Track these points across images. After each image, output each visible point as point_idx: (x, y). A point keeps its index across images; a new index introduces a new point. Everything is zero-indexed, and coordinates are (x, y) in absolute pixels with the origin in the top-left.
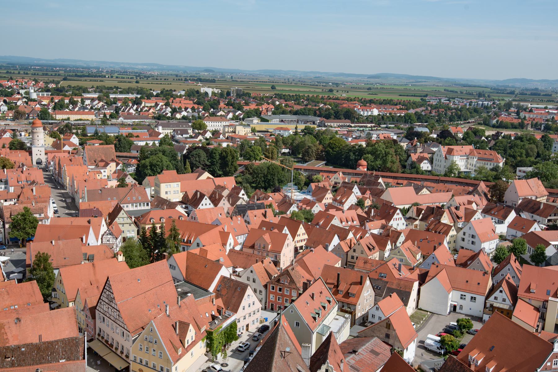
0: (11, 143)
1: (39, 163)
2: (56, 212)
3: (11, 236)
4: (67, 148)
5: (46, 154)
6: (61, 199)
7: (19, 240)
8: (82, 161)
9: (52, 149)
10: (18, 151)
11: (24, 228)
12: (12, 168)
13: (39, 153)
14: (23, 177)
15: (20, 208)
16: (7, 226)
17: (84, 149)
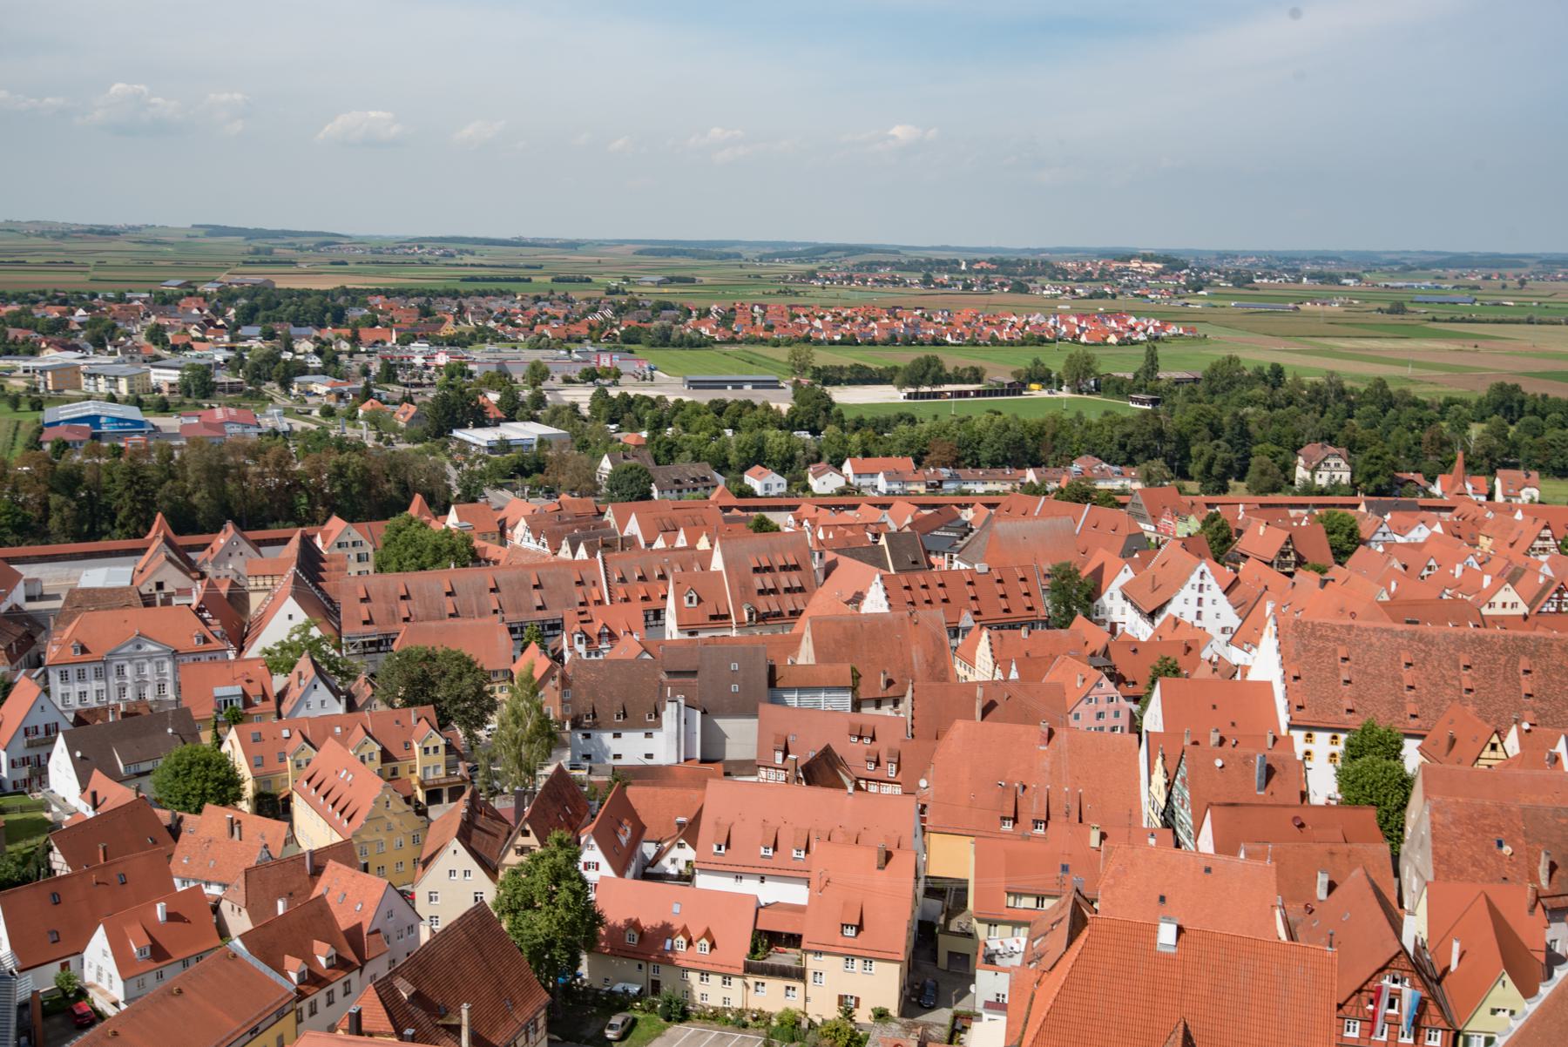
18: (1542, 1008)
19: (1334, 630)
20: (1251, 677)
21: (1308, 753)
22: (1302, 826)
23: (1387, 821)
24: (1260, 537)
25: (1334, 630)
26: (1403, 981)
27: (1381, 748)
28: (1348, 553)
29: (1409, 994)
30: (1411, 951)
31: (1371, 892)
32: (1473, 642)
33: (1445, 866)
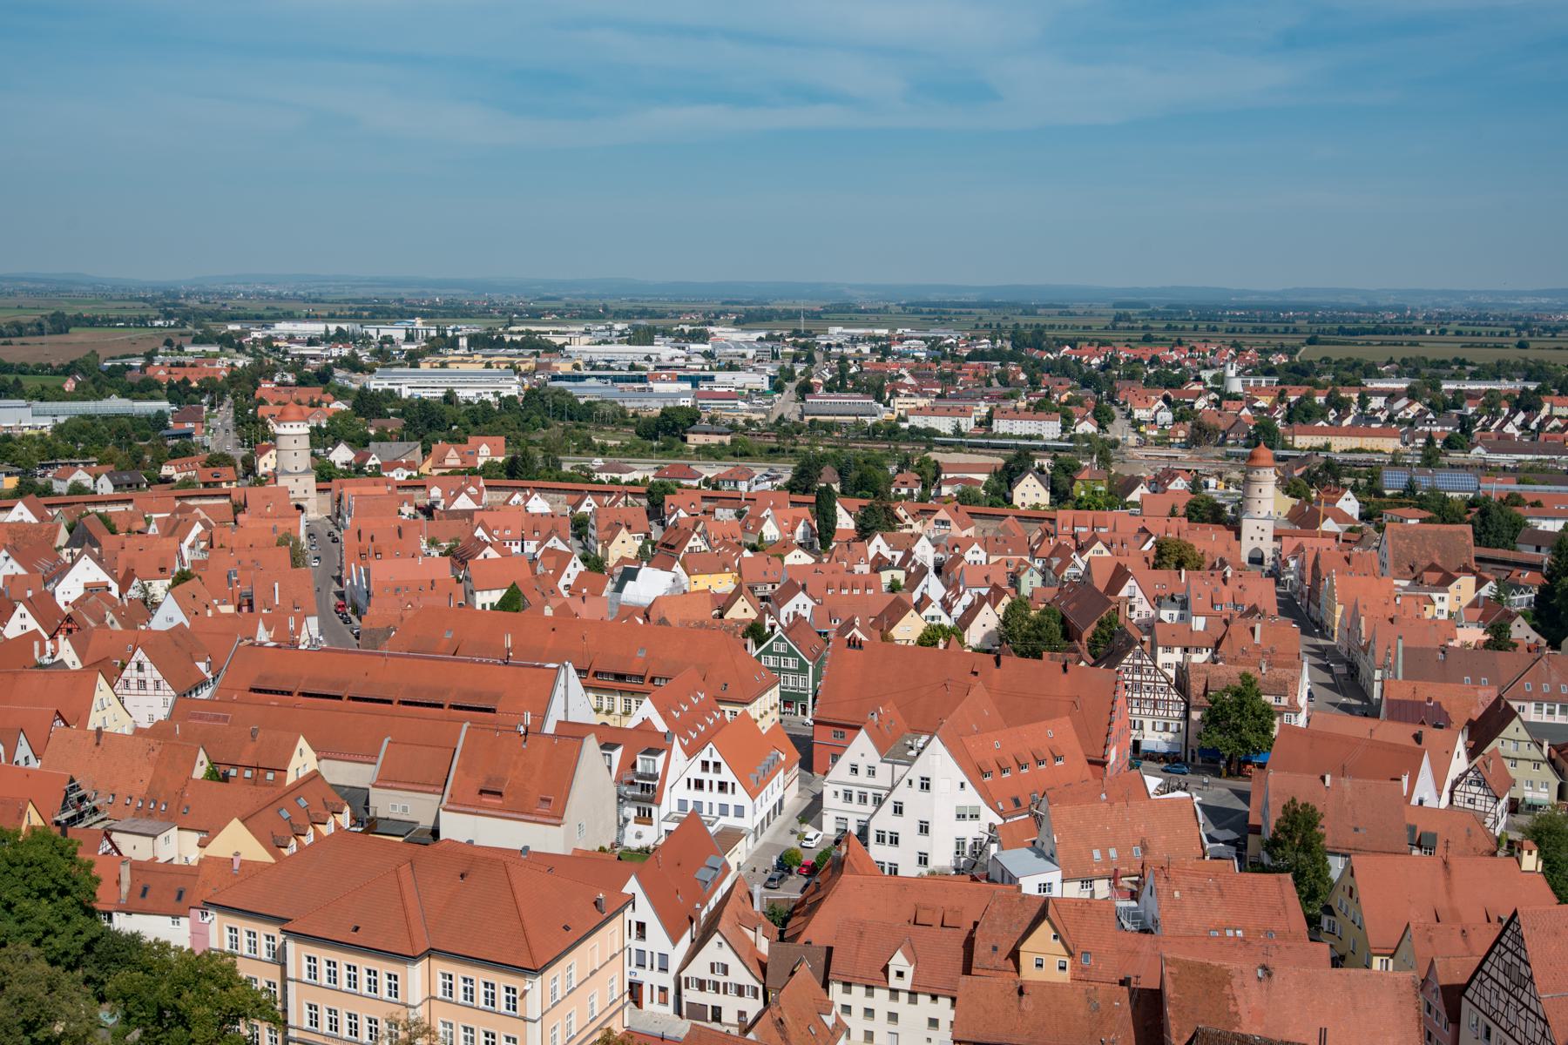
0: (1190, 503)
1: (1257, 560)
2: (1310, 694)
3: (1205, 744)
4: (1329, 525)
5: (1277, 538)
6: (1320, 661)
7: (1223, 756)
8: (1377, 567)
9: (1287, 527)
10: (1211, 528)
11: (1238, 728)
12: (1198, 568)
13: (1258, 533)
14: (1226, 593)
15: (1228, 673)
16: (1196, 715)
17: (1380, 528)
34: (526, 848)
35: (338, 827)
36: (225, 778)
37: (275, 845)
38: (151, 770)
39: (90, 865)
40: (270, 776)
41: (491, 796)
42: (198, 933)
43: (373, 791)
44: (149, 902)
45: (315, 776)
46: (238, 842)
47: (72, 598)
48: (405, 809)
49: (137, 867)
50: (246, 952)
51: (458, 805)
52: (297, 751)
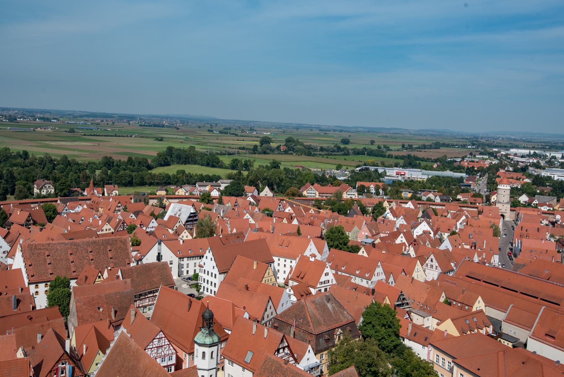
18: (107, 358)
19: (43, 246)
20: (13, 268)
21: (37, 292)
22: (31, 318)
23: (64, 310)
24: (18, 215)
25: (43, 246)
26: (66, 363)
27: (62, 285)
28: (54, 218)
29: (68, 367)
30: (69, 352)
31: (54, 336)
32: (92, 243)
33: (81, 320)
34: (558, 362)
35: (487, 332)
36: (450, 304)
37: (462, 332)
38: (426, 295)
39: (399, 320)
40: (467, 307)
41: (549, 337)
42: (429, 353)
43: (503, 323)
44: (416, 338)
45: (481, 311)
46: (449, 327)
47: (418, 234)
48: (515, 333)
49: (414, 326)
50: (441, 365)
51: (535, 336)
52: (477, 301)
